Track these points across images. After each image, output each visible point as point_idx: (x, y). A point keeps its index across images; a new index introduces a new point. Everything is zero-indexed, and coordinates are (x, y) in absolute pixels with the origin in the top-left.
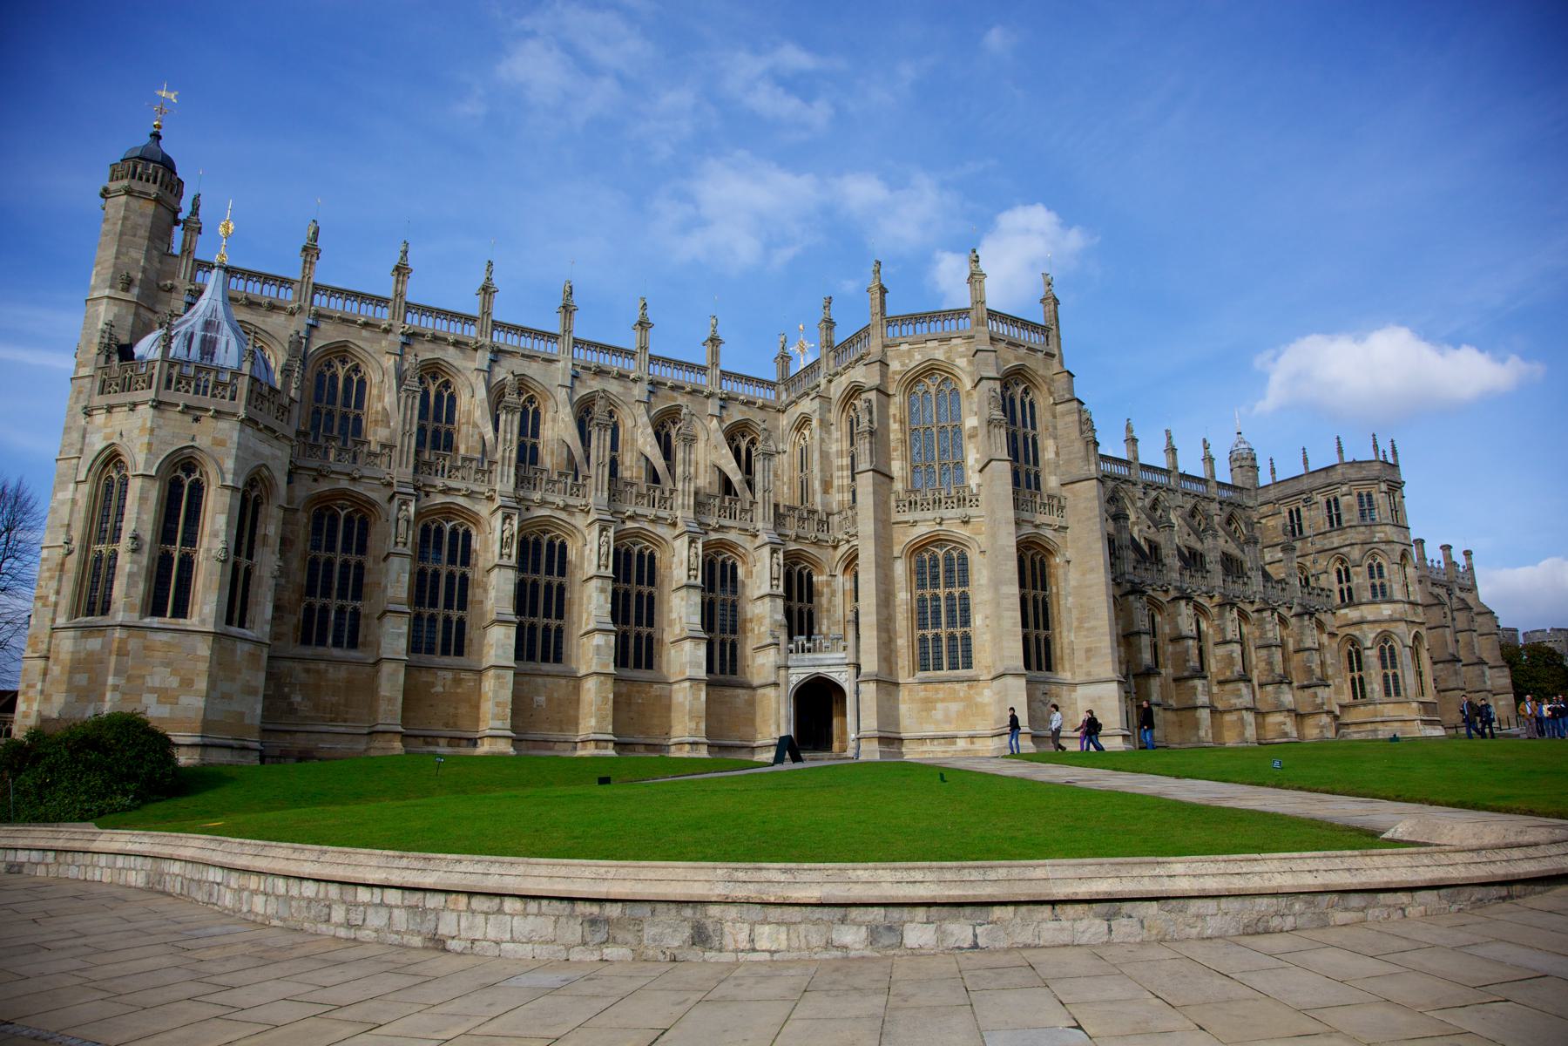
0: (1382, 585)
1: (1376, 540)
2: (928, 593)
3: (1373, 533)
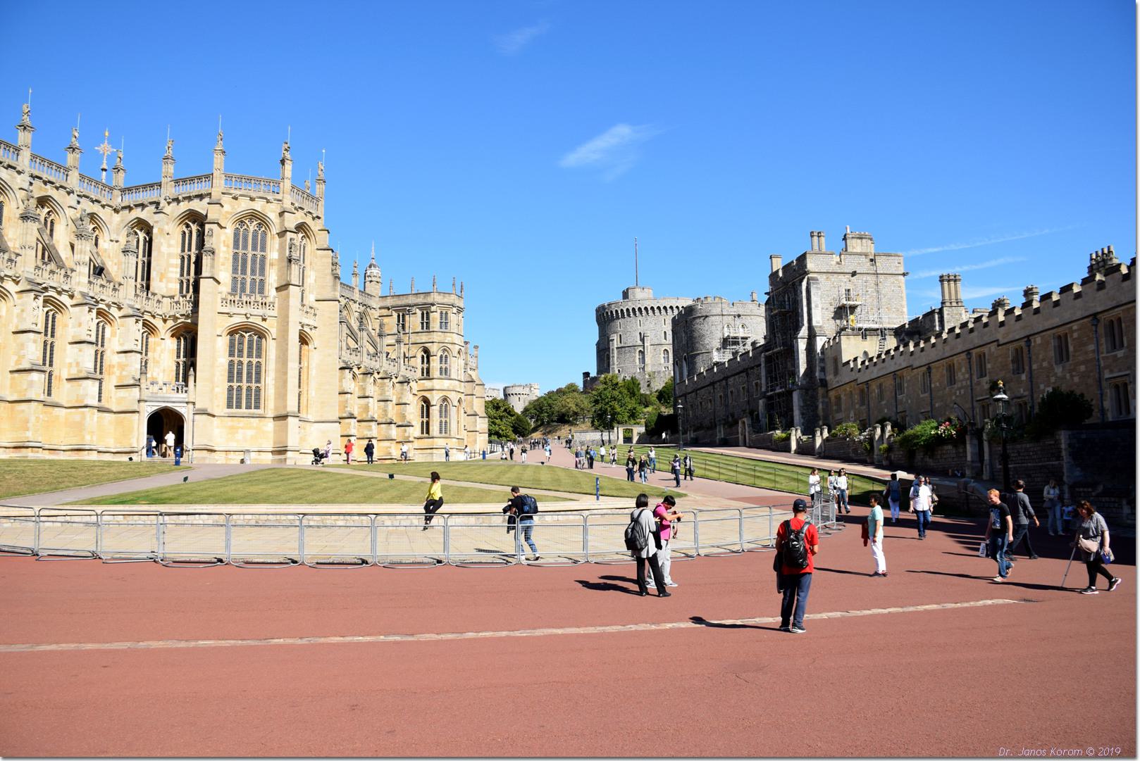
0: (446, 369)
1: (446, 341)
2: (236, 359)
3: (445, 337)
